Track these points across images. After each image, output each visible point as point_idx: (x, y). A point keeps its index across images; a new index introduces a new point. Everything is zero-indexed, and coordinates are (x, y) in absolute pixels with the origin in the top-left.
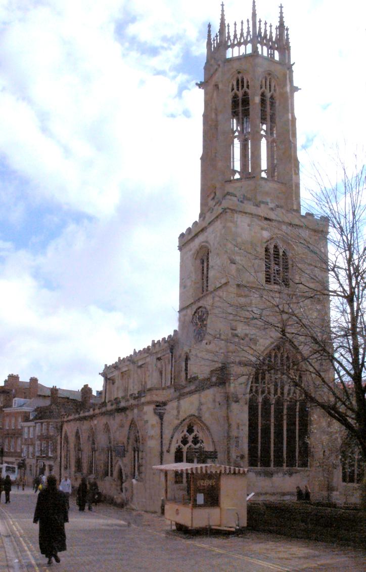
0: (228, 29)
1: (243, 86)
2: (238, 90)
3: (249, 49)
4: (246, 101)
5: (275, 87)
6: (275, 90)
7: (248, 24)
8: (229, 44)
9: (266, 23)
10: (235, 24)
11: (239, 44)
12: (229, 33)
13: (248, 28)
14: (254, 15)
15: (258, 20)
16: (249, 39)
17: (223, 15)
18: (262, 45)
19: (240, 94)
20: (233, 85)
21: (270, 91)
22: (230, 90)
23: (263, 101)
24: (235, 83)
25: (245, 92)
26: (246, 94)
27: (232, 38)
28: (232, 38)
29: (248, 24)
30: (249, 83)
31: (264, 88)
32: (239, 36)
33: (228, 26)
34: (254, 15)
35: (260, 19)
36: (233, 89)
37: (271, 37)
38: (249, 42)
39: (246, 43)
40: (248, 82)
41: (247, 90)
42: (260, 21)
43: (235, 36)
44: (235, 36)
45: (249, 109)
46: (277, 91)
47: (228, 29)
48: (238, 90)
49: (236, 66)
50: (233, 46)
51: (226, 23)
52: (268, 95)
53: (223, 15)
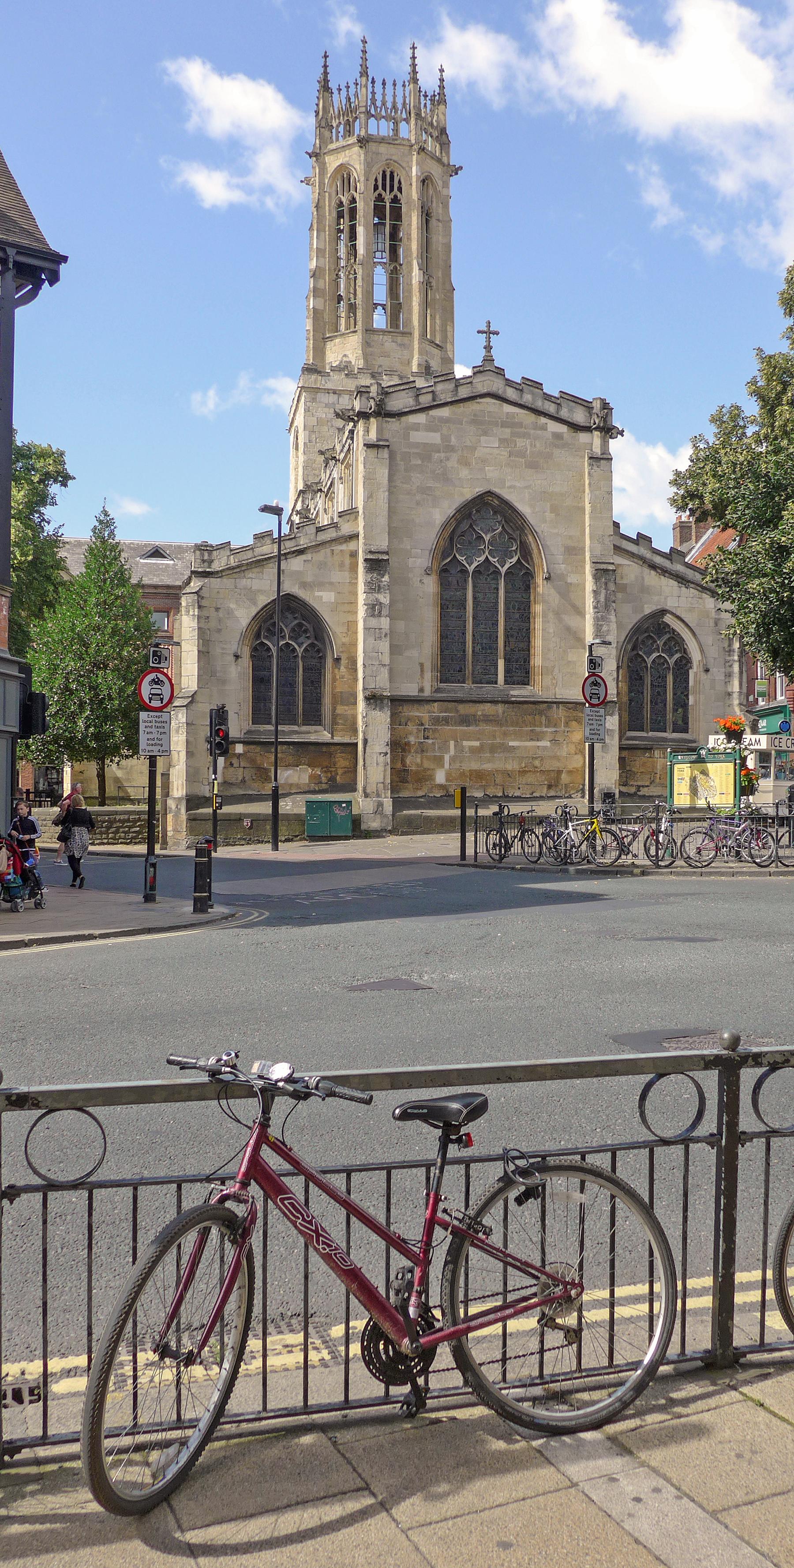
0: (373, 87)
2: (384, 189)
7: (404, 90)
19: (388, 197)
20: (376, 180)
25: (396, 196)
26: (395, 200)
28: (379, 104)
29: (404, 90)
36: (376, 188)
40: (400, 182)
41: (399, 195)
43: (384, 103)
44: (384, 103)
47: (373, 87)
48: (384, 189)
50: (378, 118)
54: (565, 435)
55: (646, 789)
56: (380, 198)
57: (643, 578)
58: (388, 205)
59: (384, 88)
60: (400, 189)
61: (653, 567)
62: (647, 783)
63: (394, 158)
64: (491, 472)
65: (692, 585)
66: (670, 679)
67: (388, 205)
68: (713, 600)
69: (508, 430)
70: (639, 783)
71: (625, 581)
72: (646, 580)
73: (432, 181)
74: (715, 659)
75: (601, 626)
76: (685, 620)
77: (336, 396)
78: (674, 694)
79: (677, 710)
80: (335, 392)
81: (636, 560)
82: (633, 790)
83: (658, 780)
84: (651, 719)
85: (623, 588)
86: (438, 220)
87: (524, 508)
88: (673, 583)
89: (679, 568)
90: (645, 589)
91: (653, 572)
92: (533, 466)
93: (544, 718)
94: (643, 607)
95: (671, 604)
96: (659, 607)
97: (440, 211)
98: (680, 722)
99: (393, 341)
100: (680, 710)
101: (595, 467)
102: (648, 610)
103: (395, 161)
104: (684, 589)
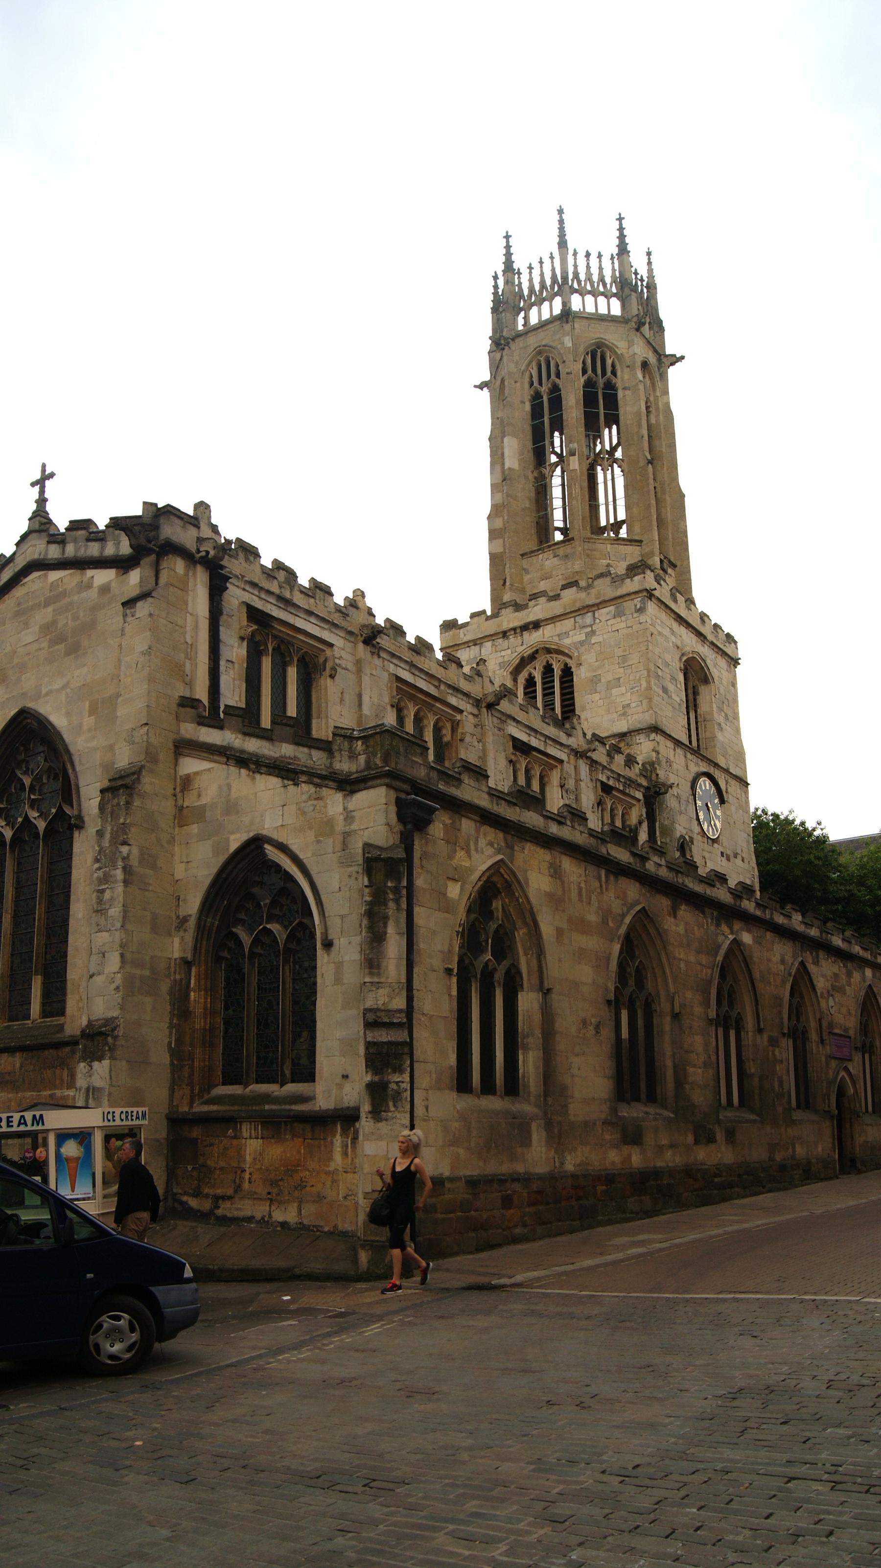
1: (549, 376)
2: (541, 384)
3: (557, 305)
4: (556, 402)
5: (613, 366)
6: (614, 373)
7: (552, 262)
8: (522, 304)
9: (588, 255)
10: (530, 268)
11: (540, 302)
12: (520, 283)
13: (553, 270)
14: (563, 244)
15: (571, 252)
16: (556, 289)
17: (508, 255)
18: (582, 293)
19: (544, 389)
20: (531, 376)
21: (604, 373)
22: (527, 386)
23: (589, 399)
24: (535, 373)
27: (526, 292)
28: (526, 292)
29: (552, 262)
30: (560, 368)
31: (590, 372)
32: (537, 287)
33: (519, 273)
34: (563, 244)
35: (575, 250)
36: (531, 384)
37: (602, 279)
38: (556, 294)
39: (551, 299)
40: (557, 366)
41: (557, 380)
42: (575, 254)
45: (562, 414)
46: (619, 373)
48: (541, 384)
49: (533, 341)
51: (515, 266)
52: (601, 382)
53: (508, 255)
54: (113, 584)
55: (228, 1204)
56: (537, 396)
57: (229, 787)
58: (545, 399)
59: (530, 273)
60: (558, 375)
61: (243, 761)
62: (230, 1192)
63: (544, 343)
64: (29, 681)
65: (303, 778)
66: (285, 974)
67: (545, 399)
68: (339, 796)
69: (50, 609)
70: (219, 1191)
71: (203, 801)
72: (234, 789)
73: (611, 349)
74: (342, 917)
75: (102, 892)
76: (294, 848)
77: (478, 647)
78: (296, 1003)
79: (300, 1036)
80: (476, 642)
81: (216, 758)
82: (207, 1205)
83: (246, 1185)
84: (258, 1058)
85: (200, 814)
86: (625, 389)
87: (58, 720)
88: (274, 782)
89: (286, 750)
90: (231, 807)
91: (244, 772)
92: (74, 650)
93: (66, 1072)
94: (227, 840)
95: (270, 824)
96: (251, 834)
97: (626, 377)
98: (304, 1061)
99: (554, 557)
100: (305, 1034)
101: (129, 619)
102: (235, 842)
103: (544, 346)
104: (292, 788)
